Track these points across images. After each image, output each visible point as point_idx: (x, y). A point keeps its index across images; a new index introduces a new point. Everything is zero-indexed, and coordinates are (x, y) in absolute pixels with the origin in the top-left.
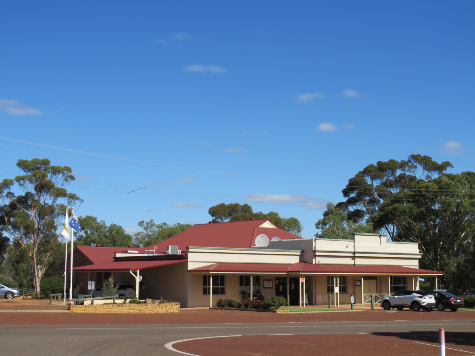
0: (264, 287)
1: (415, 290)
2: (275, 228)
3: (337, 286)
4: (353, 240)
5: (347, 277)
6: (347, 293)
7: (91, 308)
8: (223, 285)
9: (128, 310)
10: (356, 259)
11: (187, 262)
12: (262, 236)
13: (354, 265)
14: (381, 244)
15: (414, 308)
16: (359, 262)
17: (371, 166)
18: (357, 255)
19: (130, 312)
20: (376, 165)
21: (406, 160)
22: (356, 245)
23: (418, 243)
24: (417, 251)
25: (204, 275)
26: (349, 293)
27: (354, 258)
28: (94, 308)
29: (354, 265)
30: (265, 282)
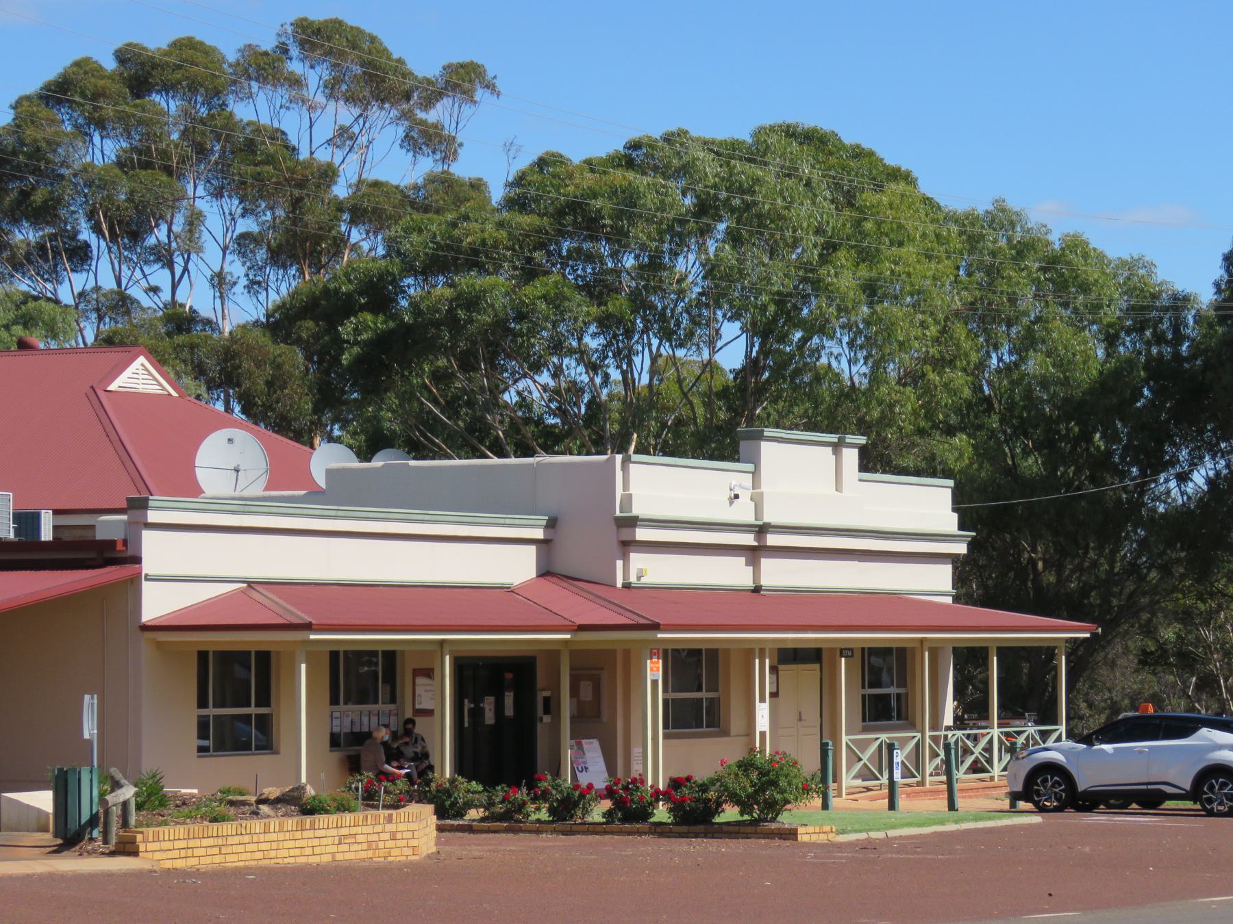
0: (418, 707)
1: (1160, 713)
2: (170, 395)
3: (762, 700)
4: (750, 467)
5: (727, 652)
6: (725, 733)
7: (210, 842)
8: (268, 704)
9: (333, 849)
10: (766, 563)
11: (134, 582)
12: (230, 440)
13: (757, 590)
14: (838, 486)
15: (1210, 801)
16: (777, 574)
17: (84, 66)
18: (772, 540)
19: (339, 857)
20: (110, 64)
21: (268, 44)
22: (765, 488)
23: (951, 483)
24: (949, 521)
25: (458, 655)
26: (733, 732)
27: (754, 554)
28: (220, 841)
29: (757, 590)
30: (420, 681)
